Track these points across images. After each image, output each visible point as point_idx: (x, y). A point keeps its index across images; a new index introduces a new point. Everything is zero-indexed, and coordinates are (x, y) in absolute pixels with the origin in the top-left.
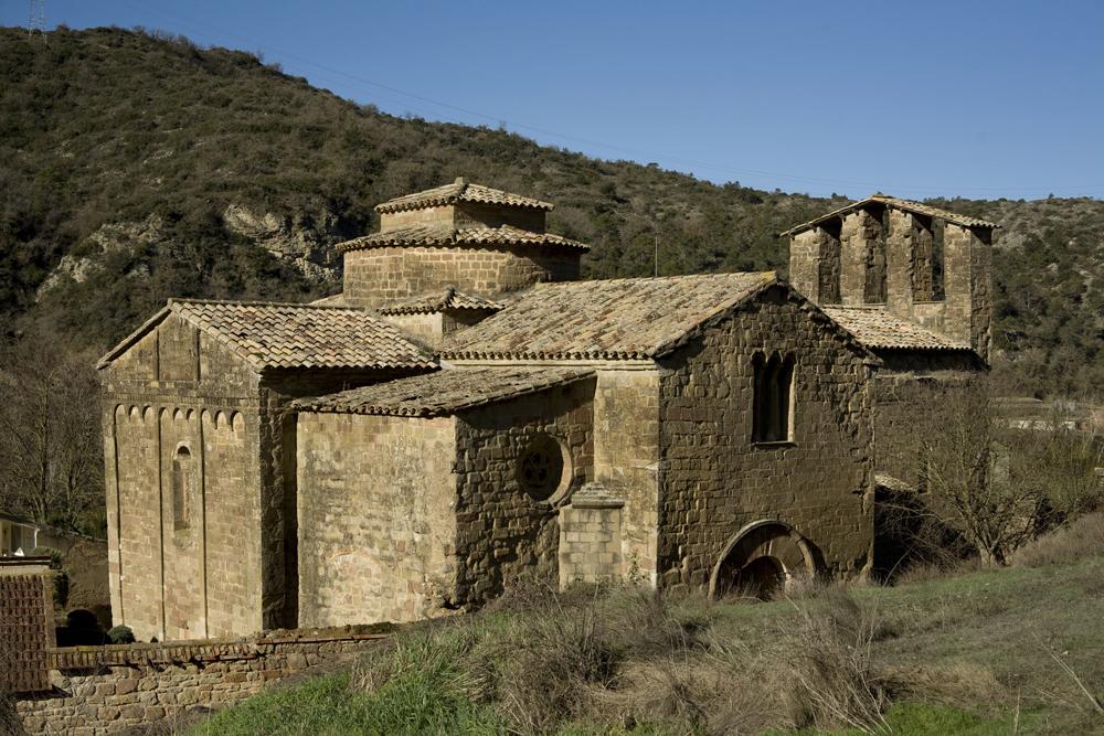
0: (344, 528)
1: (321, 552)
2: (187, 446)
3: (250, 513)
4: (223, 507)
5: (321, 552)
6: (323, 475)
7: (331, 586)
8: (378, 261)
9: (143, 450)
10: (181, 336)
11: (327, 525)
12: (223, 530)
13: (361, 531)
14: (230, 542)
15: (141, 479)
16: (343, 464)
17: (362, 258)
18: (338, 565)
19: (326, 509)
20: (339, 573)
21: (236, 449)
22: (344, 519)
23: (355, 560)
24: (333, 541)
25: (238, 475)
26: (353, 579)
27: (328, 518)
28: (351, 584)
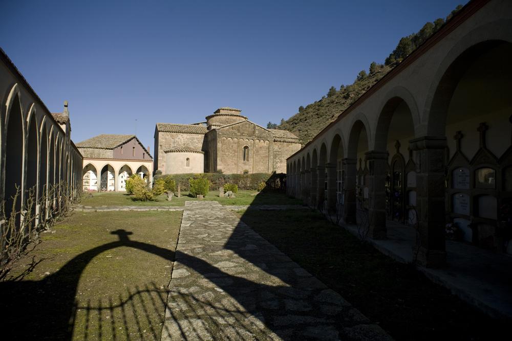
9: (232, 146)
12: (260, 160)
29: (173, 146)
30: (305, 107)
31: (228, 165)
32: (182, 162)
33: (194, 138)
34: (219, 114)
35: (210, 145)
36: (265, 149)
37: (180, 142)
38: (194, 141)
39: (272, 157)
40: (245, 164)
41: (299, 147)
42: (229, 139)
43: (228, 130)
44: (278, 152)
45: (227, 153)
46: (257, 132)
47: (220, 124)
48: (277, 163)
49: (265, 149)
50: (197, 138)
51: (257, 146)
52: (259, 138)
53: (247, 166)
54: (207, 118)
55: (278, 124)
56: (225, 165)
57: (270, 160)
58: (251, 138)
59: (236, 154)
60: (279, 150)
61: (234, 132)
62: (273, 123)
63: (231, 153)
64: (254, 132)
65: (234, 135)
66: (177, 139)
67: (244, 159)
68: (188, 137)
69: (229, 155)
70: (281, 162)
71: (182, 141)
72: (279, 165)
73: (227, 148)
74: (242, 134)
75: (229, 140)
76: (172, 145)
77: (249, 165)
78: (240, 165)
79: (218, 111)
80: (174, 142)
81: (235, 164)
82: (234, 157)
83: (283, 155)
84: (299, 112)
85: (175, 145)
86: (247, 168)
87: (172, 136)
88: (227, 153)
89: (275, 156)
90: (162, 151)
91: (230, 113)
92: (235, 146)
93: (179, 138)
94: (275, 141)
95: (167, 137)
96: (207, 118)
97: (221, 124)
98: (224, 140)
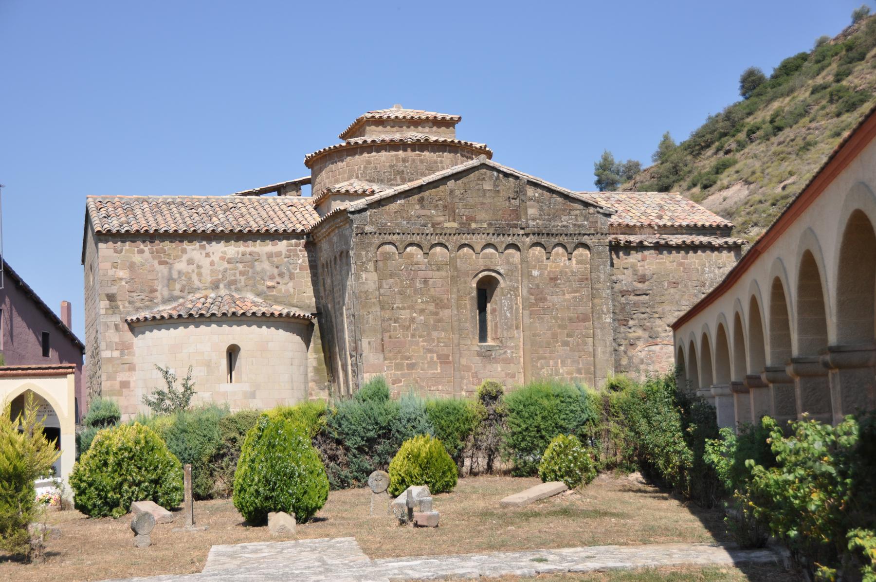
3: (599, 318)
4: (556, 318)
6: (624, 293)
9: (426, 281)
10: (495, 186)
12: (555, 336)
14: (566, 344)
15: (423, 306)
18: (642, 355)
21: (572, 272)
24: (638, 338)
25: (576, 292)
27: (631, 323)
29: (166, 293)
30: (768, 73)
31: (412, 367)
32: (208, 364)
33: (255, 258)
34: (360, 140)
35: (328, 281)
36: (575, 285)
37: (195, 278)
38: (258, 266)
39: (608, 319)
40: (486, 355)
41: (735, 264)
45: (405, 314)
46: (532, 211)
47: (366, 186)
49: (575, 285)
50: (270, 256)
51: (535, 273)
52: (545, 238)
53: (499, 367)
54: (310, 163)
55: (647, 162)
56: (398, 367)
57: (598, 332)
58: (509, 240)
59: (445, 313)
61: (430, 217)
62: (621, 159)
63: (422, 311)
64: (517, 213)
65: (429, 230)
69: (413, 320)
70: (653, 338)
71: (206, 271)
72: (640, 352)
73: (400, 293)
74: (465, 229)
75: (411, 255)
77: (507, 361)
78: (464, 361)
79: (359, 127)
80: (170, 280)
81: (444, 360)
82: (435, 328)
84: (741, 99)
86: (494, 374)
87: (154, 254)
88: (405, 314)
89: (622, 318)
90: (117, 319)
91: (412, 134)
92: (438, 278)
93: (190, 262)
94: (615, 248)
95: (137, 258)
96: (310, 163)
97: (375, 187)
98: (387, 257)
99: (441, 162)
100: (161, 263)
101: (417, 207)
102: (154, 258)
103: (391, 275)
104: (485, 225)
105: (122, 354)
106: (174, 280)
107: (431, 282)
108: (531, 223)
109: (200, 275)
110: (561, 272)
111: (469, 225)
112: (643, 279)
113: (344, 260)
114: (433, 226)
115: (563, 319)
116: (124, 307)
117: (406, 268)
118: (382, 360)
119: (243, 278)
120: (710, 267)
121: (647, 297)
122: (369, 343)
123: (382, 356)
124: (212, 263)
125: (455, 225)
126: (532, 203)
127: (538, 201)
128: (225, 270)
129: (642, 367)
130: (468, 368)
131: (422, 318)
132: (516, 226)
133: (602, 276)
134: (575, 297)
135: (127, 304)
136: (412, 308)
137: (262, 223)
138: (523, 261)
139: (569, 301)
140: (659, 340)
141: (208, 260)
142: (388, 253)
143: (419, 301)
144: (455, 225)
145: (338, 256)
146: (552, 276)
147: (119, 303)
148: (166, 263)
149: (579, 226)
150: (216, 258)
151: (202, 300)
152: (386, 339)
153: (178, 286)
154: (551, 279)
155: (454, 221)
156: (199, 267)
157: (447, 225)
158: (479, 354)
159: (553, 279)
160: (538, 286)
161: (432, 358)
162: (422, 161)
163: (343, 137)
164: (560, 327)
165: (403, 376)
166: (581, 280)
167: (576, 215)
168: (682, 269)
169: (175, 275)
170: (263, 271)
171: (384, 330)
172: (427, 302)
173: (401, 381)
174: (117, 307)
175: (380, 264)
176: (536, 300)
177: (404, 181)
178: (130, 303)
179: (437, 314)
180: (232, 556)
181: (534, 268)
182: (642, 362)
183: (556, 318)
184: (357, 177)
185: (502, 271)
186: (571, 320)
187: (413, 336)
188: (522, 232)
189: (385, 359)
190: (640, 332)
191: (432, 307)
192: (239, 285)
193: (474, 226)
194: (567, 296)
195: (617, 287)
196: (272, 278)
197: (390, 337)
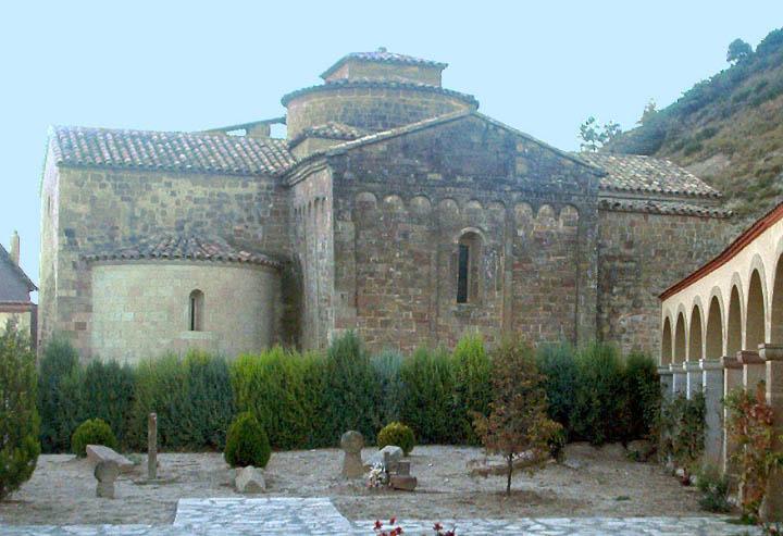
0: (629, 297)
1: (605, 316)
2: (478, 231)
3: (584, 284)
4: (539, 281)
5: (605, 316)
6: (609, 258)
7: (620, 340)
8: (423, 103)
9: (405, 235)
11: (614, 295)
12: (537, 299)
13: (652, 298)
16: (633, 250)
17: (401, 97)
19: (615, 283)
20: (628, 330)
21: (559, 234)
22: (632, 291)
23: (644, 318)
24: (622, 306)
26: (642, 332)
27: (615, 290)
28: (641, 335)
29: (128, 233)
31: (386, 324)
37: (158, 217)
42: (389, 199)
43: (385, 157)
44: (621, 258)
45: (381, 268)
48: (615, 313)
49: (560, 247)
50: (239, 197)
51: (521, 233)
56: (371, 323)
58: (495, 195)
59: (423, 270)
60: (627, 252)
61: (413, 167)
63: (399, 266)
66: (145, 203)
67: (462, 299)
68: (199, 192)
69: (389, 275)
75: (390, 206)
76: (125, 230)
82: (412, 284)
83: (644, 276)
85: (138, 232)
88: (381, 268)
92: (418, 232)
93: (155, 199)
95: (98, 192)
98: (365, 206)
99: (426, 109)
100: (123, 199)
101: (400, 155)
102: (116, 193)
103: (370, 226)
104: (471, 179)
105: (79, 294)
106: (136, 218)
107: (410, 236)
108: (519, 180)
109: (164, 213)
110: (548, 233)
111: (455, 177)
112: (630, 245)
113: (319, 207)
114: (416, 175)
115: (546, 282)
116: (83, 244)
117: (385, 219)
118: (354, 315)
119: (209, 221)
120: (698, 236)
121: (633, 265)
122: (342, 296)
123: (354, 310)
124: (177, 203)
125: (440, 177)
126: (521, 158)
127: (528, 157)
128: (191, 210)
129: (624, 336)
130: (445, 329)
131: (399, 273)
132: (503, 182)
133: (589, 240)
134: (558, 261)
135: (86, 241)
136: (388, 261)
137: (231, 162)
138: (509, 218)
139: (553, 264)
140: (642, 309)
141: (175, 199)
142: (367, 203)
143: (398, 255)
144: (440, 177)
145: (313, 203)
146: (537, 236)
147: (78, 239)
148: (128, 200)
149: (569, 186)
150: (182, 196)
151: (165, 241)
152: (361, 292)
153: (140, 225)
154: (537, 240)
155: (438, 172)
156: (163, 205)
157: (430, 176)
158: (457, 314)
159: (539, 240)
160: (522, 247)
161: (407, 316)
162: (405, 107)
163: (323, 76)
164: (542, 290)
165: (376, 332)
166: (569, 242)
167: (566, 176)
168: (670, 237)
169: (138, 214)
170: (232, 215)
171: (359, 283)
172: (404, 256)
173: (373, 339)
174: (76, 244)
175: (358, 214)
176: (519, 260)
177: (386, 127)
178: (89, 239)
179: (415, 269)
180: (204, 509)
181: (519, 227)
182: (624, 331)
183: (539, 281)
184: (336, 120)
185: (486, 229)
186: (554, 283)
187: (389, 291)
188: (508, 188)
189: (358, 314)
190: (624, 300)
191: (410, 263)
192: (205, 228)
193: (459, 179)
194: (552, 259)
195: (603, 252)
196: (241, 221)
197: (364, 291)
